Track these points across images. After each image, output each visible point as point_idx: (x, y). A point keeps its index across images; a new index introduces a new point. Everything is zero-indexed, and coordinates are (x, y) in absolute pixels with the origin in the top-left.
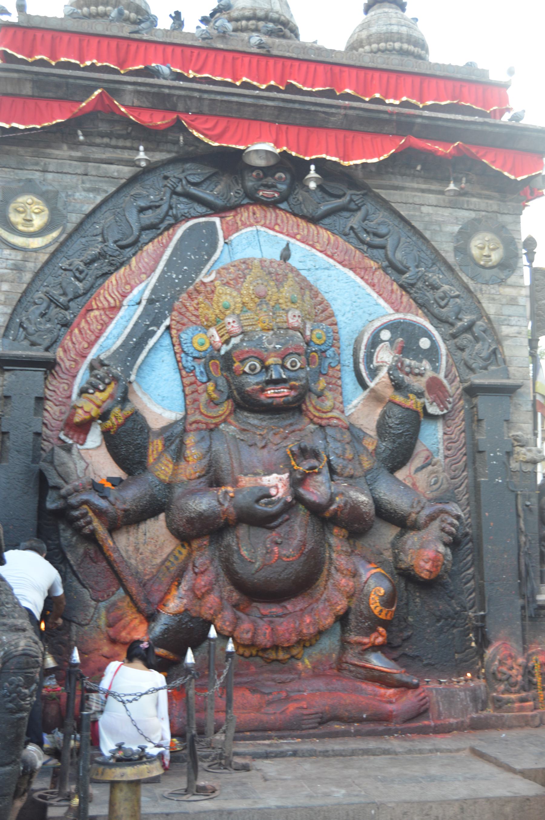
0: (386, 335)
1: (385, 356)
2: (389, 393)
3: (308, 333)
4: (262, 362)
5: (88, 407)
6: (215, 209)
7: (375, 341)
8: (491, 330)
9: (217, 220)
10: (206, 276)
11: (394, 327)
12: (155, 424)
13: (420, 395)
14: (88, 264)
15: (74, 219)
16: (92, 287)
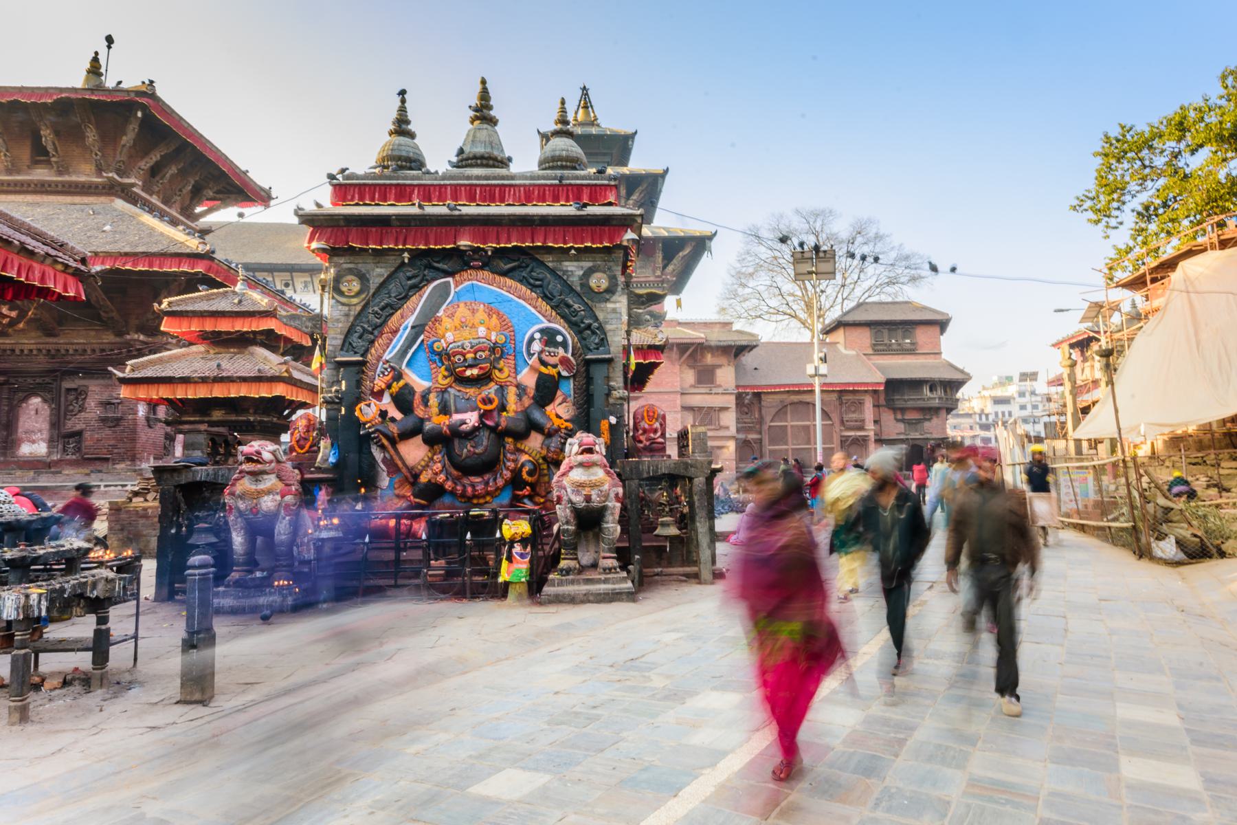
0: (537, 336)
1: (536, 347)
2: (538, 365)
3: (493, 338)
4: (464, 355)
5: (379, 383)
6: (451, 274)
7: (532, 339)
8: (601, 328)
9: (450, 279)
10: (441, 313)
11: (542, 331)
12: (418, 390)
13: (555, 366)
14: (382, 309)
15: (373, 287)
16: (385, 322)
